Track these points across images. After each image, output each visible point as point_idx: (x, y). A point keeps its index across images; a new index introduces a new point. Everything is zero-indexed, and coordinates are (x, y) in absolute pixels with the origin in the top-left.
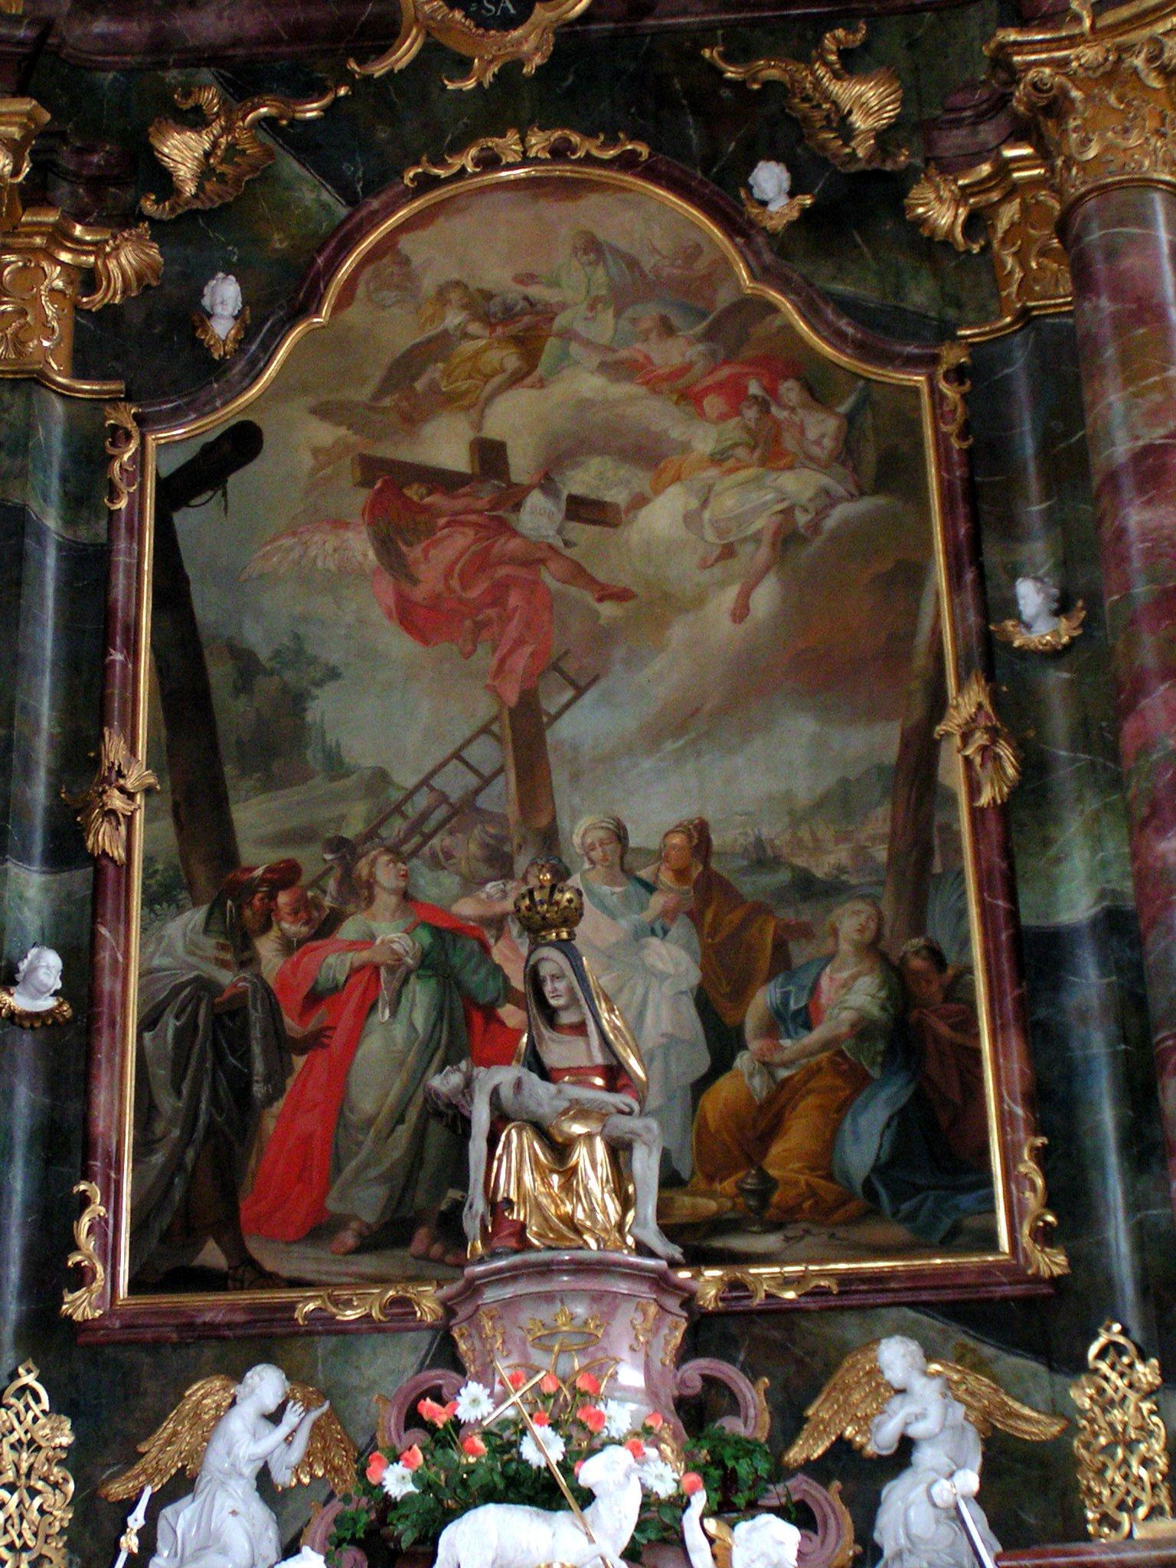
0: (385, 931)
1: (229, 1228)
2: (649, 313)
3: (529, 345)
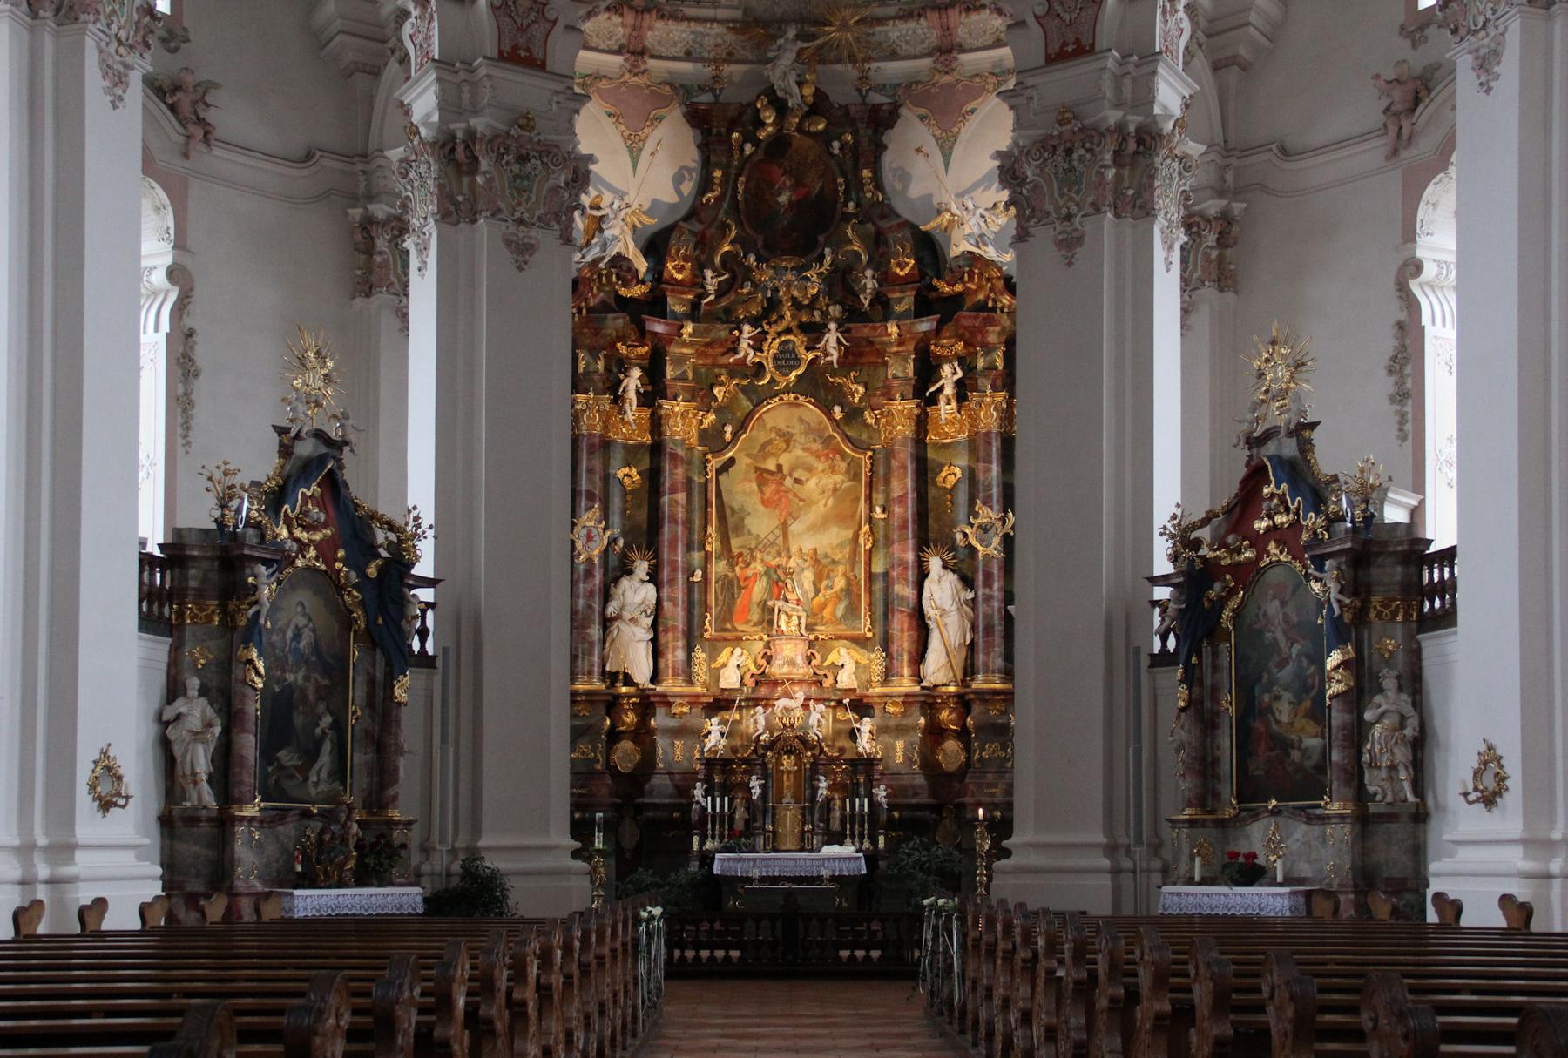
0: (758, 567)
1: (731, 621)
2: (811, 437)
3: (788, 442)
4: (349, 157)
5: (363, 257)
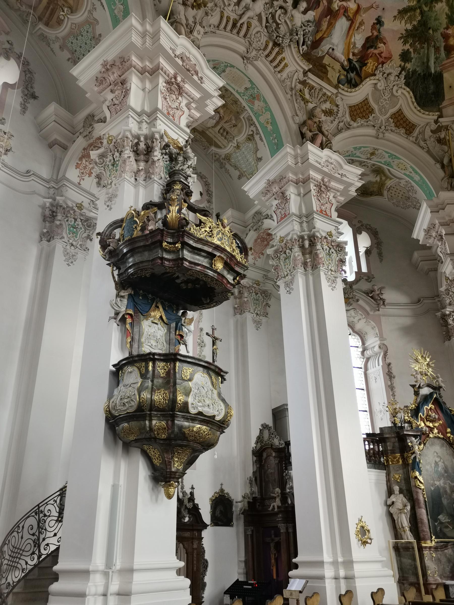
4: (433, 298)
5: (445, 328)
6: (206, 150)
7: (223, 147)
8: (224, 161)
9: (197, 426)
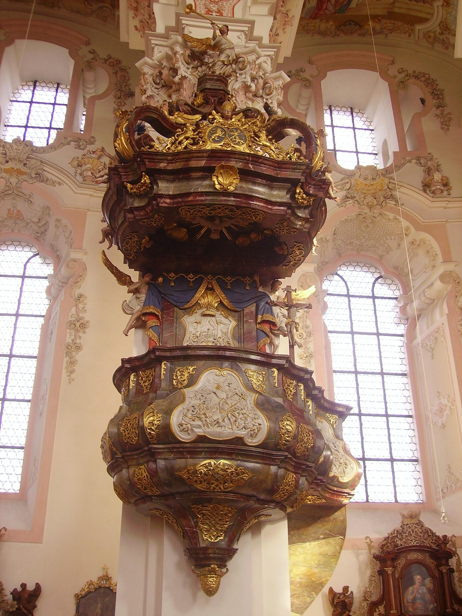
6: (412, 35)
7: (429, 16)
8: (444, 36)
9: (204, 464)
